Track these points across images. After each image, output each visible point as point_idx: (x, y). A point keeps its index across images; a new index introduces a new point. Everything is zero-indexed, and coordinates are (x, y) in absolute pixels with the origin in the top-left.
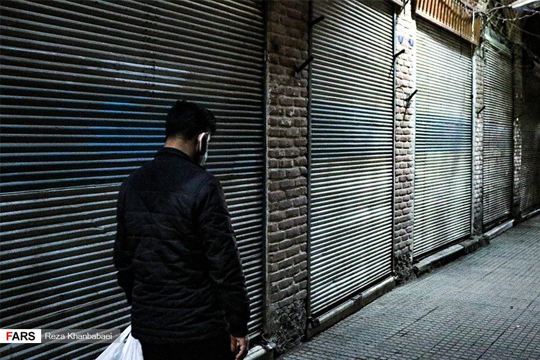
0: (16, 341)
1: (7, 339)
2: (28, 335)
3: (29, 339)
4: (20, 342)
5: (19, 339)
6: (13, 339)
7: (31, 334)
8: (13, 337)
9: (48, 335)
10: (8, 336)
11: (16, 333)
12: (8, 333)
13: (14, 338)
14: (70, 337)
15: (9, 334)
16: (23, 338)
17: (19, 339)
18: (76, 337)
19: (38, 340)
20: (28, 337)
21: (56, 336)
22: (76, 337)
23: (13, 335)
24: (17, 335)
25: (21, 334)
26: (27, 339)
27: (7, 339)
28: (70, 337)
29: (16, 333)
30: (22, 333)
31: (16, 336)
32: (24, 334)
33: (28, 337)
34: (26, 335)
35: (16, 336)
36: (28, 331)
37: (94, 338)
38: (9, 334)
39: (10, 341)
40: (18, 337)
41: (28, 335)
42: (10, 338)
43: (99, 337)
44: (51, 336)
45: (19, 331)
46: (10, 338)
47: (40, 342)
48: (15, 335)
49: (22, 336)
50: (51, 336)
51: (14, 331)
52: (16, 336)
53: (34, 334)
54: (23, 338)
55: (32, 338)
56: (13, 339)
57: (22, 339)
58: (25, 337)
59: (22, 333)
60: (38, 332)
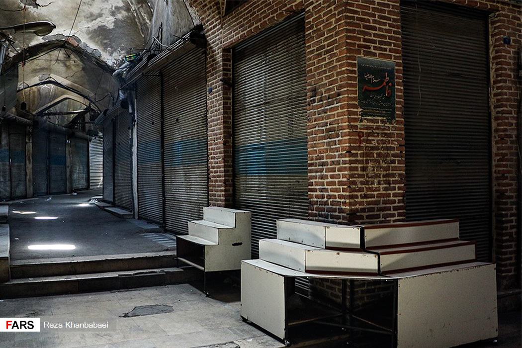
0: (15, 330)
1: (7, 328)
2: (27, 324)
3: (28, 327)
4: (20, 330)
5: (18, 328)
6: (13, 328)
7: (30, 323)
8: (12, 325)
9: (47, 323)
10: (7, 325)
11: (15, 322)
12: (7, 322)
13: (14, 326)
14: (67, 326)
15: (9, 323)
16: (22, 326)
17: (18, 328)
18: (73, 325)
19: (37, 329)
20: (27, 325)
21: (55, 325)
22: (73, 325)
23: (12, 323)
24: (17, 324)
25: (21, 323)
26: (26, 328)
27: (7, 328)
28: (67, 326)
29: (15, 322)
30: (21, 322)
31: (15, 325)
32: (23, 323)
33: (27, 325)
34: (26, 324)
35: (15, 325)
36: (27, 320)
37: (91, 326)
38: (9, 323)
39: (10, 329)
40: (17, 326)
41: (27, 324)
42: (10, 327)
43: (95, 326)
44: (49, 325)
45: (18, 320)
46: (10, 327)
47: (38, 330)
48: (14, 324)
49: (21, 325)
50: (49, 325)
51: (13, 320)
52: (15, 325)
53: (33, 322)
54: (22, 326)
55: (31, 327)
56: (13, 328)
57: (21, 328)
58: (24, 325)
59: (21, 322)
60: (36, 321)
